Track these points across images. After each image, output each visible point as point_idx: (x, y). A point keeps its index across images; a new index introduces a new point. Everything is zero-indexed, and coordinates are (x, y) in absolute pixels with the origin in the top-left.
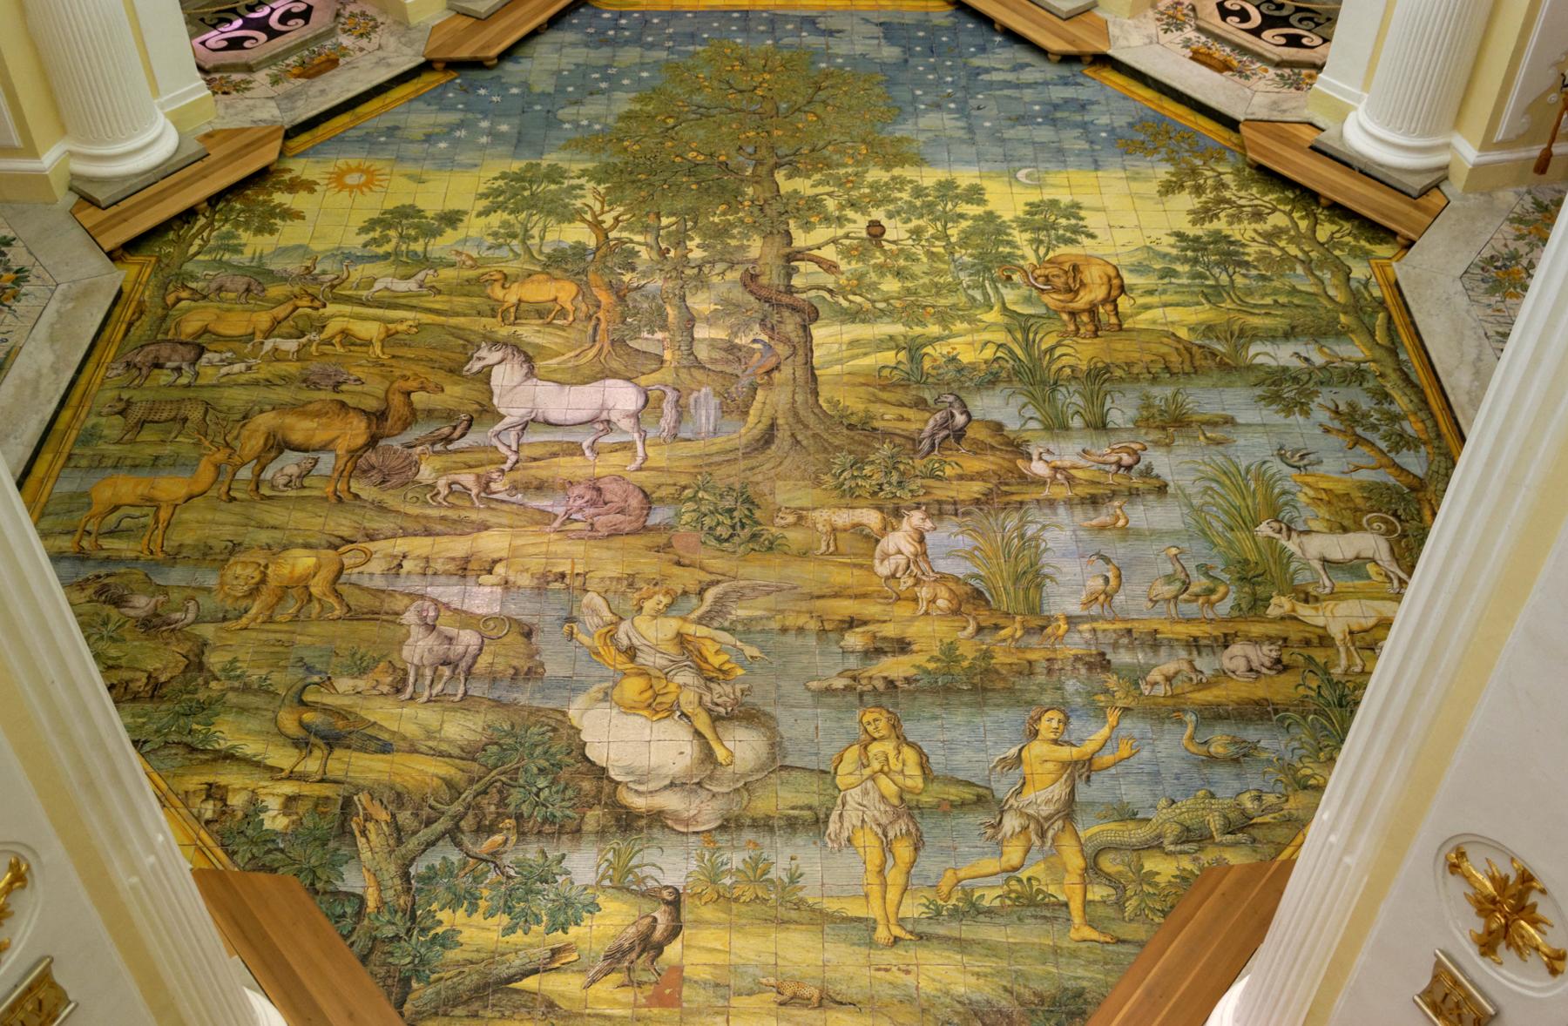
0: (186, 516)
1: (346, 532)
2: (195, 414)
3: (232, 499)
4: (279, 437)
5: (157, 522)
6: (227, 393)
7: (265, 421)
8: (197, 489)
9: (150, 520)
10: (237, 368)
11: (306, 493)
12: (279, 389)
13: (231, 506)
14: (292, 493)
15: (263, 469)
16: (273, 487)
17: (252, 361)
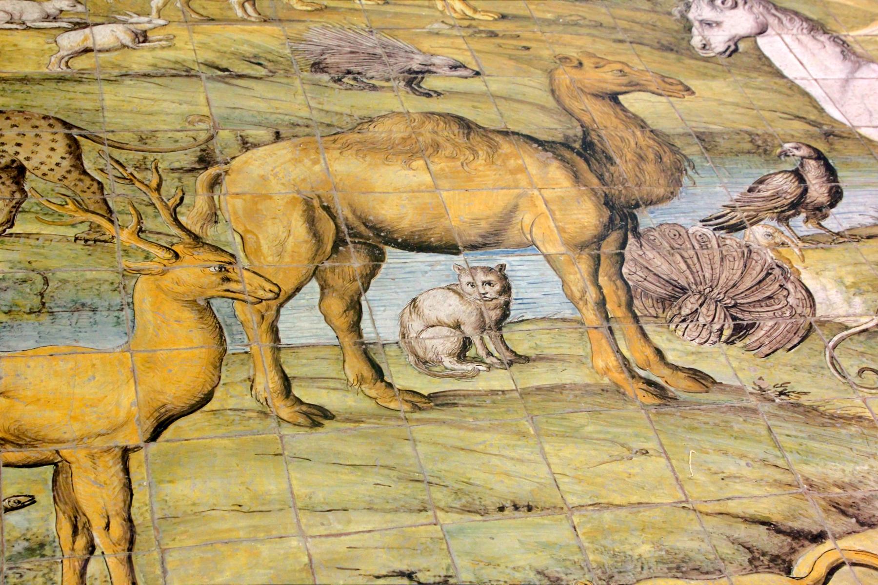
0: (183, 491)
1: (770, 506)
2: (45, 154)
3: (317, 416)
4: (343, 212)
5: (78, 525)
6: (110, 95)
7: (270, 173)
8: (176, 389)
9: (43, 520)
10: (104, 35)
11: (539, 376)
12: (259, 88)
13: (325, 437)
14: (499, 380)
15: (355, 307)
16: (424, 364)
17: (142, 23)
